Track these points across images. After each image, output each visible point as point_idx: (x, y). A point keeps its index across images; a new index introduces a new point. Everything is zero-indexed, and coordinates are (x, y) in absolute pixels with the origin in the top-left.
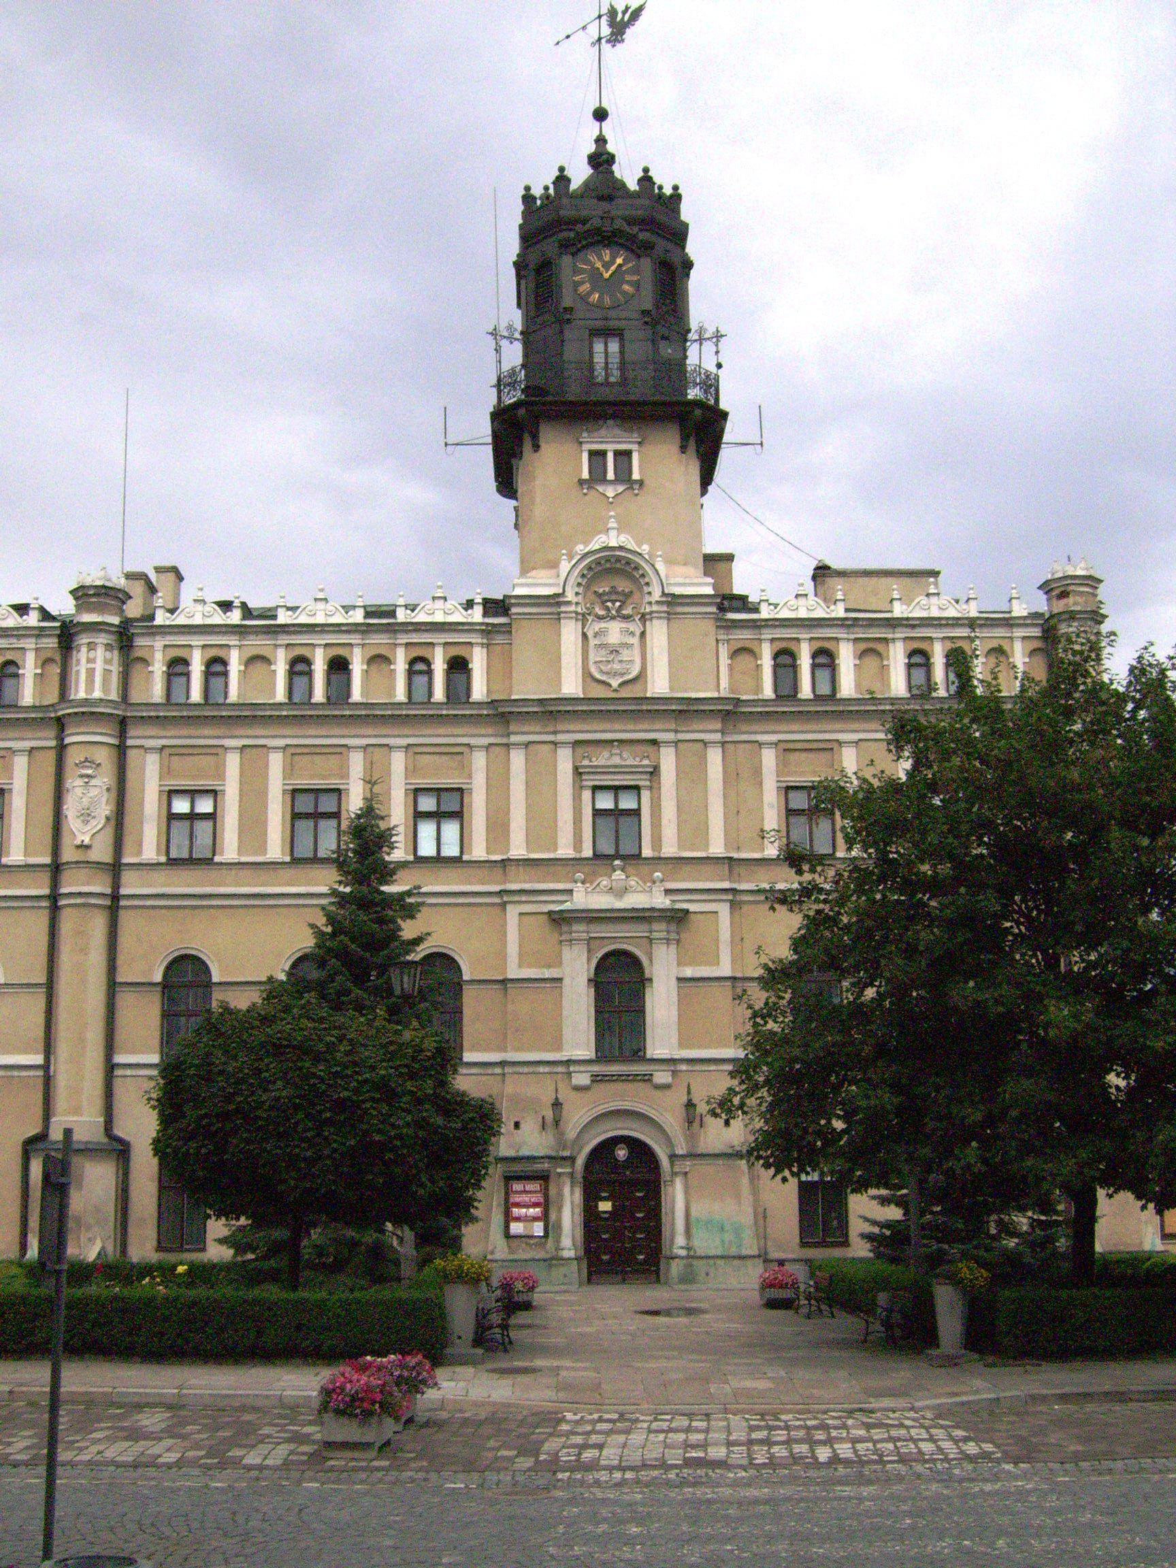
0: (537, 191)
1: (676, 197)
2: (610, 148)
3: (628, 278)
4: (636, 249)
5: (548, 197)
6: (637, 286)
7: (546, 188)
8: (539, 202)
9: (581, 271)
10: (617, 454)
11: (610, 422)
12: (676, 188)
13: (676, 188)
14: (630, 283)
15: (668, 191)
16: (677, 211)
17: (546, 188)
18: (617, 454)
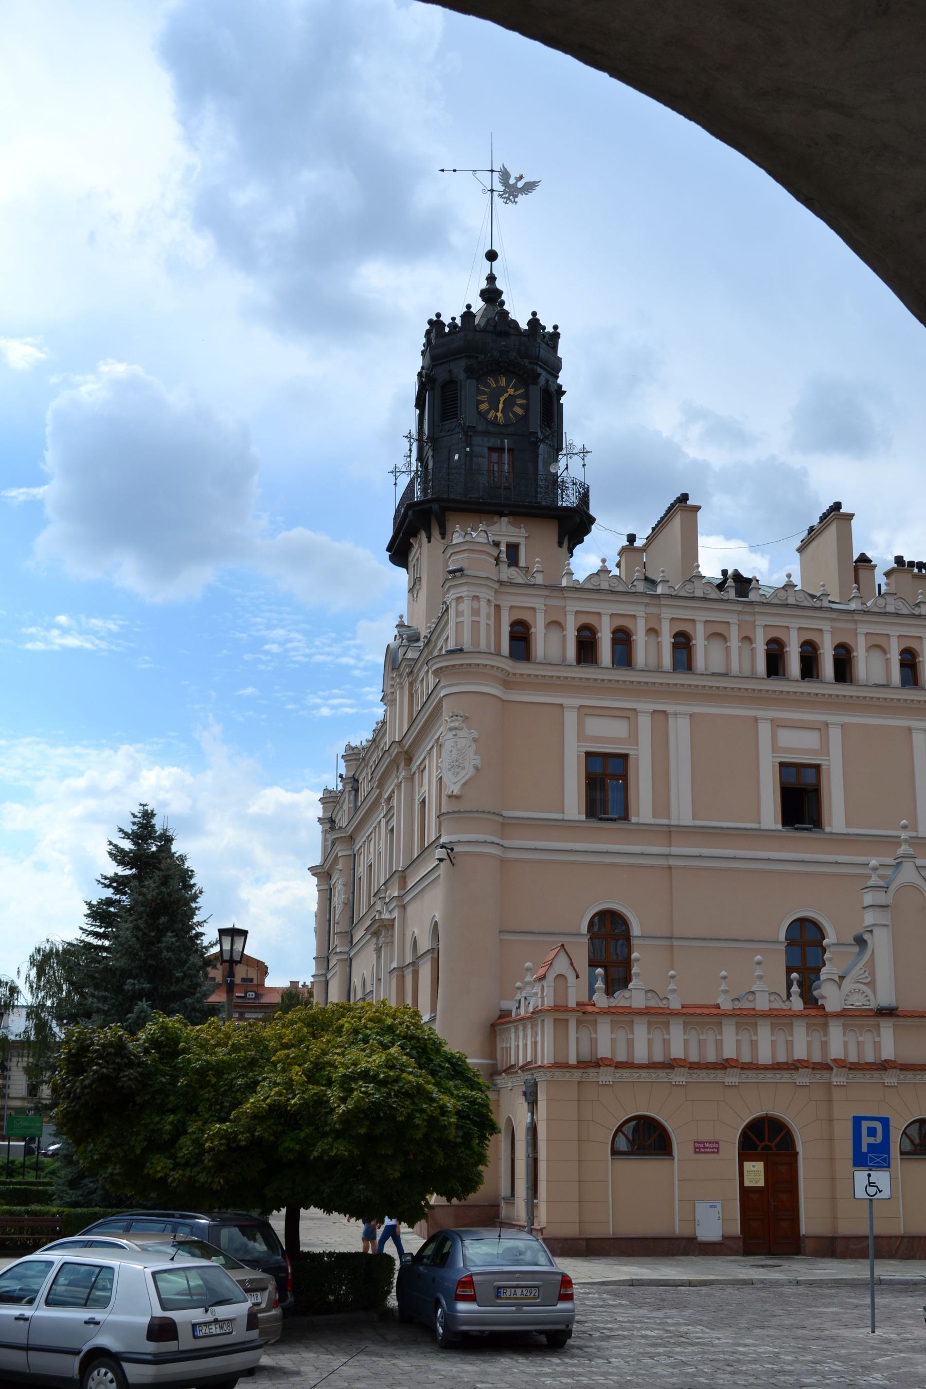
0: (446, 320)
1: (555, 336)
2: (499, 285)
3: (519, 401)
4: (526, 378)
5: (456, 326)
6: (526, 408)
7: (453, 319)
8: (447, 330)
9: (484, 393)
10: (509, 546)
11: (505, 520)
12: (556, 327)
13: (556, 327)
14: (521, 406)
15: (549, 329)
16: (555, 348)
17: (453, 319)
18: (509, 546)
